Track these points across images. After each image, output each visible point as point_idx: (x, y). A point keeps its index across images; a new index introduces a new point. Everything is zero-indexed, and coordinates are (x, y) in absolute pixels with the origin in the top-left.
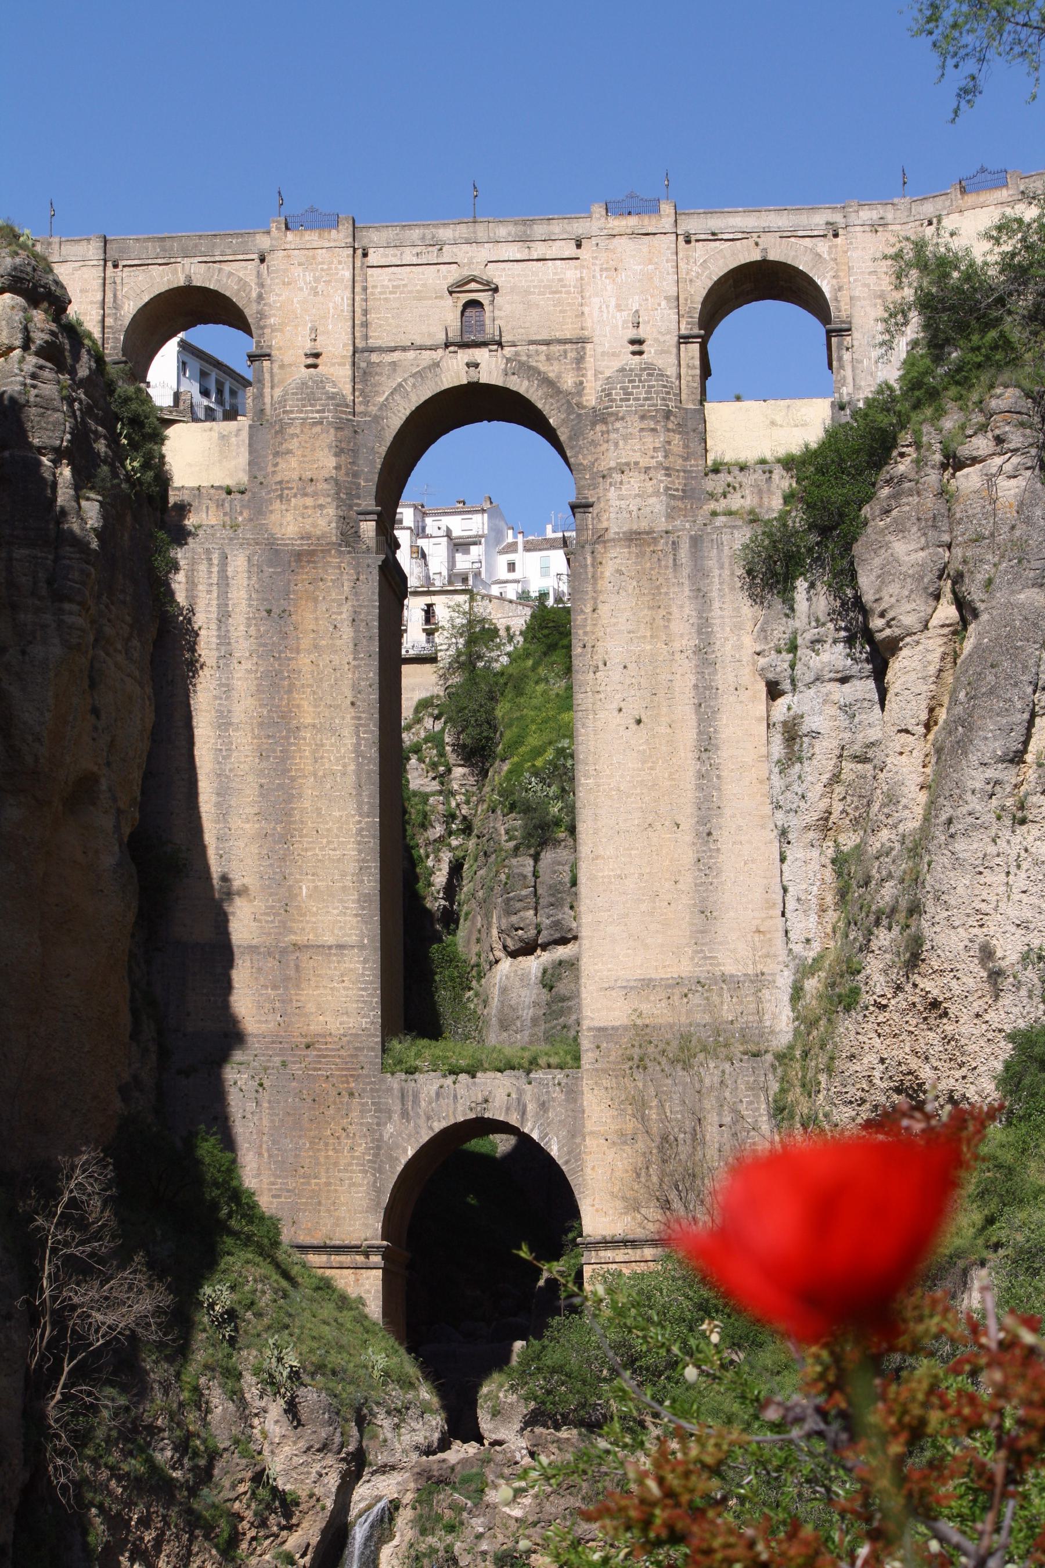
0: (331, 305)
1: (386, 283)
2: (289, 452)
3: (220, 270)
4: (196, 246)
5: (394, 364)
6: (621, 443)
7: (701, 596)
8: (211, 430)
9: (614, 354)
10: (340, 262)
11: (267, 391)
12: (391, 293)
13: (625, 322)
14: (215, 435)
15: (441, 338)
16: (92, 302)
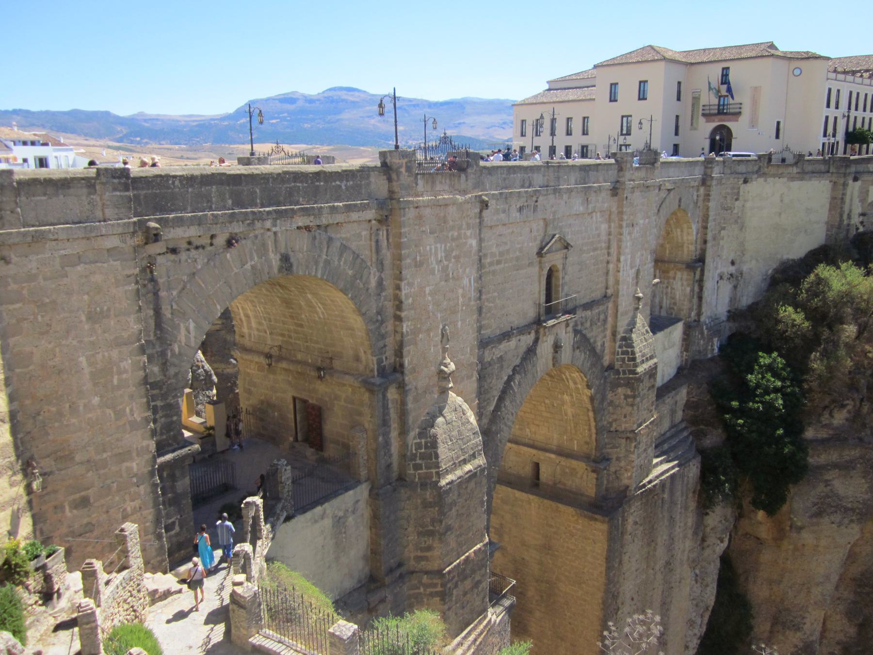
0: (460, 291)
1: (494, 249)
2: (449, 528)
3: (330, 240)
4: (290, 193)
5: (501, 359)
6: (640, 404)
7: (672, 519)
8: (322, 517)
9: (626, 313)
10: (468, 228)
11: (394, 434)
12: (499, 262)
13: (633, 278)
14: (328, 522)
15: (531, 314)
16: (118, 343)
